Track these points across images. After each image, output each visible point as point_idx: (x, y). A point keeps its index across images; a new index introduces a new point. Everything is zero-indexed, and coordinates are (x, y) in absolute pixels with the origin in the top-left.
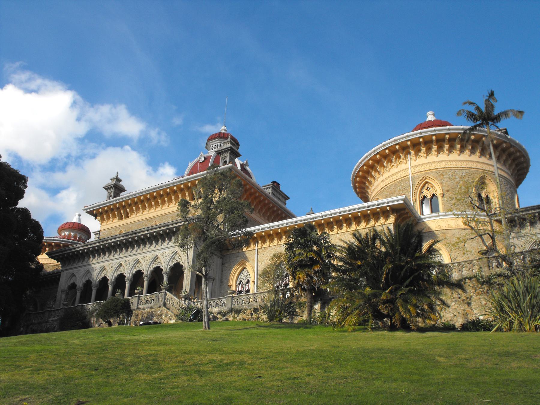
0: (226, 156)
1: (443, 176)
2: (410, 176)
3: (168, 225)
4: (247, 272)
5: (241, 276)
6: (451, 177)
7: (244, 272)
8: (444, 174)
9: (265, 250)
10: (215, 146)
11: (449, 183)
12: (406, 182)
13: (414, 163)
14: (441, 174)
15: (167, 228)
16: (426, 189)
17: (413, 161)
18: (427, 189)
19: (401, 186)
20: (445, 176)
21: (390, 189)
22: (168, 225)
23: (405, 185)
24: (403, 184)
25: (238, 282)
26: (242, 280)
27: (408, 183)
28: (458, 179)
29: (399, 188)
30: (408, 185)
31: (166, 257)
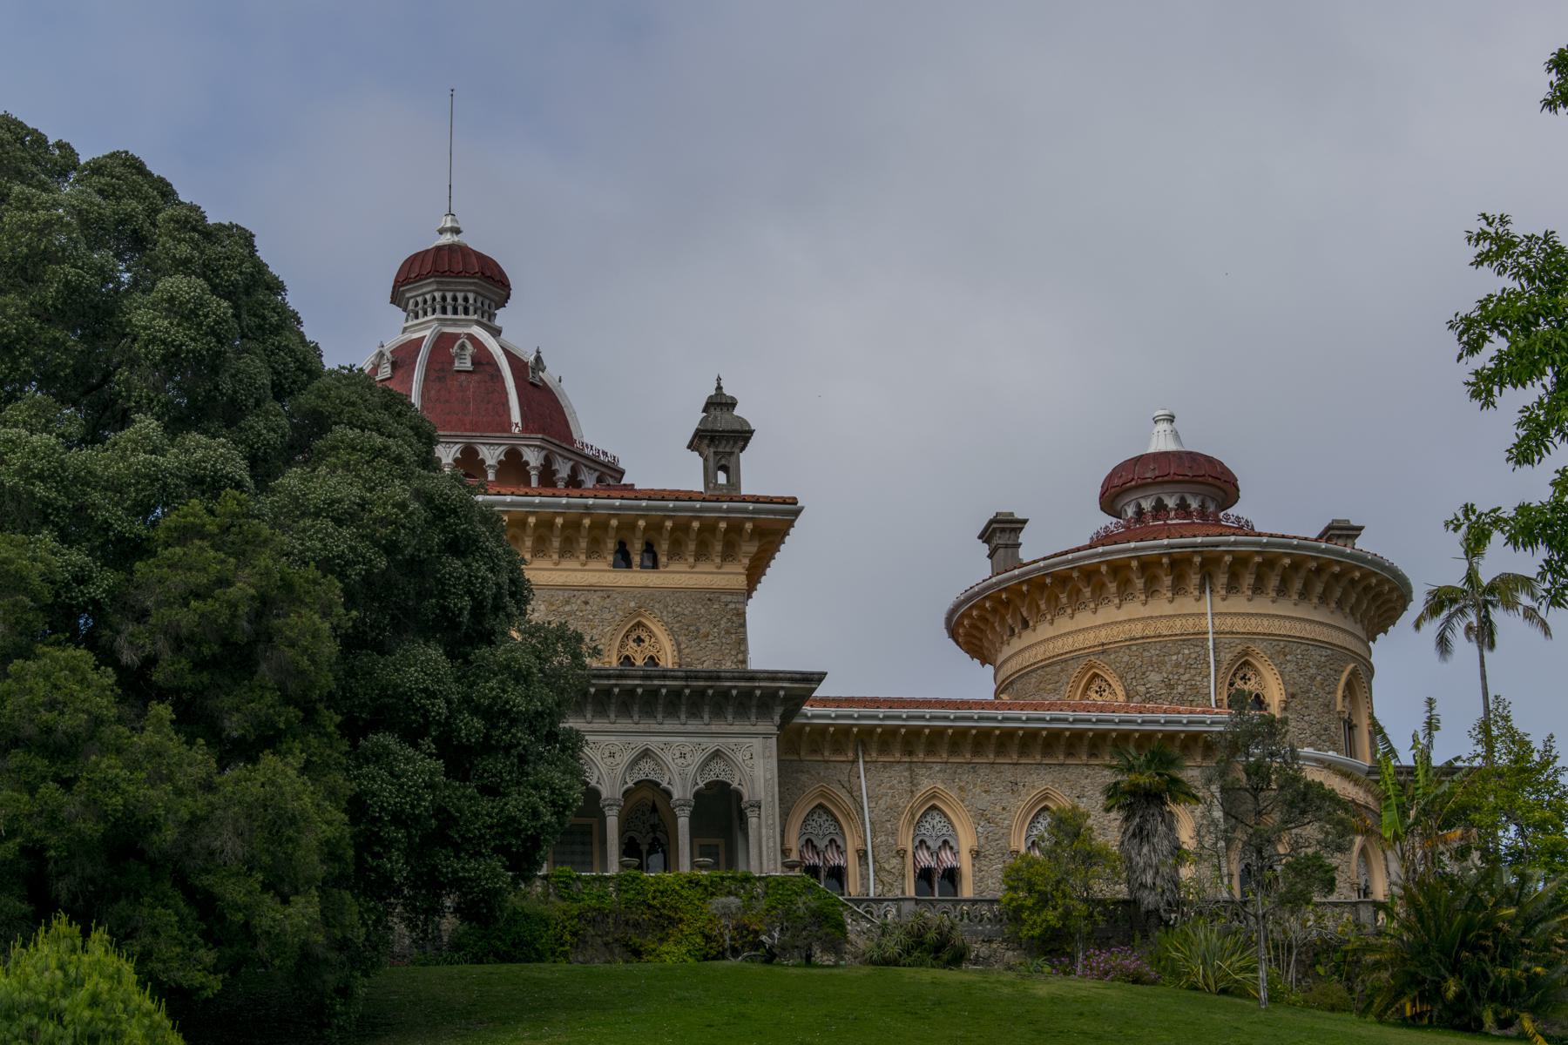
0: (728, 450)
1: (1285, 656)
2: (1210, 636)
3: (719, 678)
5: (809, 827)
6: (1300, 661)
7: (815, 817)
8: (1287, 650)
9: (885, 767)
11: (1296, 675)
12: (1198, 649)
13: (1222, 607)
14: (1282, 647)
15: (713, 684)
16: (1241, 679)
17: (1217, 600)
20: (1288, 658)
21: (1146, 654)
22: (719, 678)
23: (1193, 656)
24: (1186, 652)
27: (1203, 652)
28: (1313, 671)
29: (1174, 657)
30: (1202, 657)
31: (682, 760)
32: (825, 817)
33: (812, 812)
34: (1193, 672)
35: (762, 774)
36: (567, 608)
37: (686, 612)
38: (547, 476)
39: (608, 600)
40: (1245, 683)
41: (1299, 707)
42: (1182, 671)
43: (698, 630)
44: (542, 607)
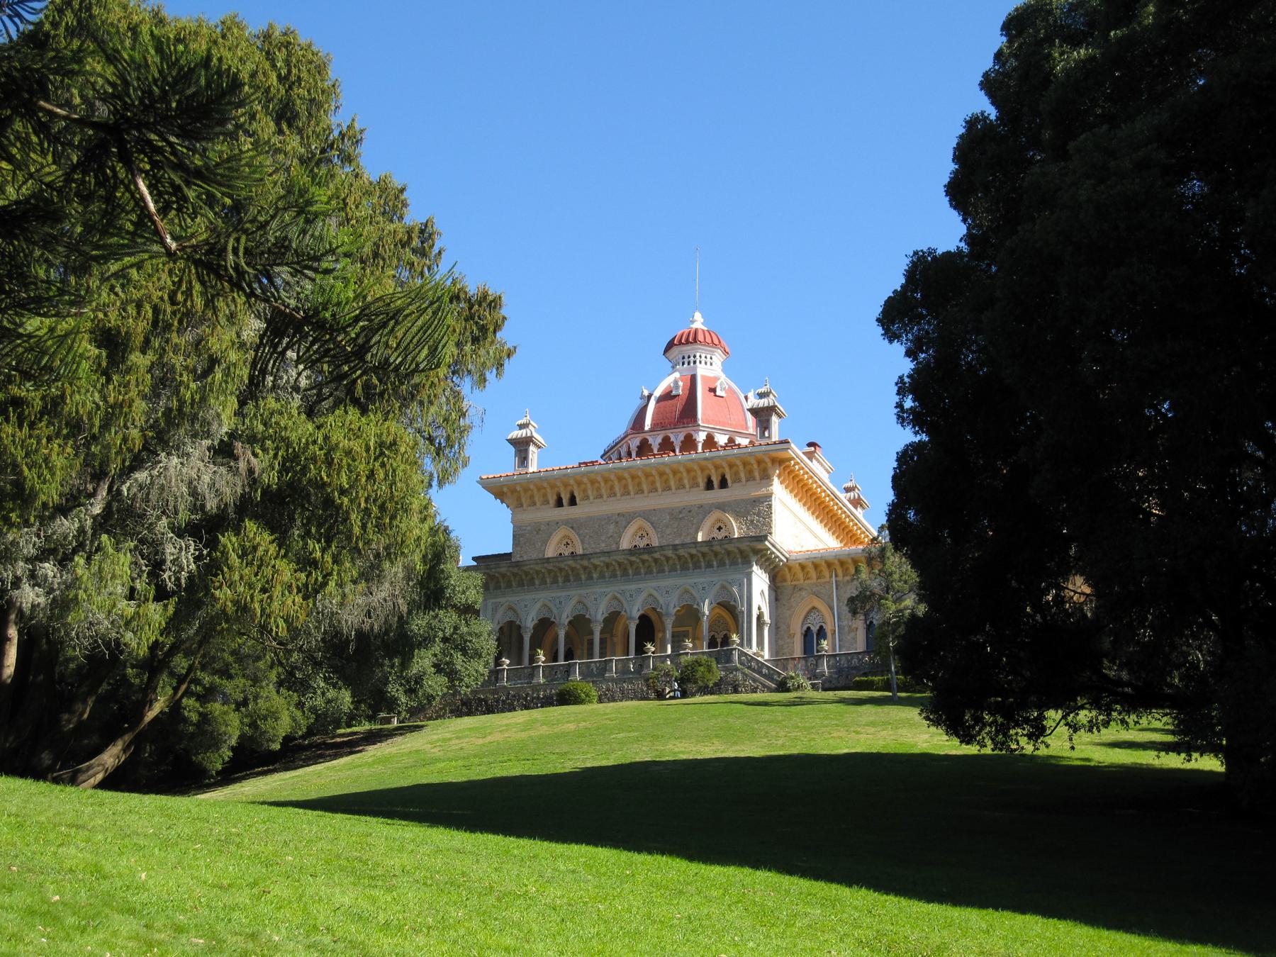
25: (805, 628)
36: (680, 516)
37: (742, 510)
38: (710, 442)
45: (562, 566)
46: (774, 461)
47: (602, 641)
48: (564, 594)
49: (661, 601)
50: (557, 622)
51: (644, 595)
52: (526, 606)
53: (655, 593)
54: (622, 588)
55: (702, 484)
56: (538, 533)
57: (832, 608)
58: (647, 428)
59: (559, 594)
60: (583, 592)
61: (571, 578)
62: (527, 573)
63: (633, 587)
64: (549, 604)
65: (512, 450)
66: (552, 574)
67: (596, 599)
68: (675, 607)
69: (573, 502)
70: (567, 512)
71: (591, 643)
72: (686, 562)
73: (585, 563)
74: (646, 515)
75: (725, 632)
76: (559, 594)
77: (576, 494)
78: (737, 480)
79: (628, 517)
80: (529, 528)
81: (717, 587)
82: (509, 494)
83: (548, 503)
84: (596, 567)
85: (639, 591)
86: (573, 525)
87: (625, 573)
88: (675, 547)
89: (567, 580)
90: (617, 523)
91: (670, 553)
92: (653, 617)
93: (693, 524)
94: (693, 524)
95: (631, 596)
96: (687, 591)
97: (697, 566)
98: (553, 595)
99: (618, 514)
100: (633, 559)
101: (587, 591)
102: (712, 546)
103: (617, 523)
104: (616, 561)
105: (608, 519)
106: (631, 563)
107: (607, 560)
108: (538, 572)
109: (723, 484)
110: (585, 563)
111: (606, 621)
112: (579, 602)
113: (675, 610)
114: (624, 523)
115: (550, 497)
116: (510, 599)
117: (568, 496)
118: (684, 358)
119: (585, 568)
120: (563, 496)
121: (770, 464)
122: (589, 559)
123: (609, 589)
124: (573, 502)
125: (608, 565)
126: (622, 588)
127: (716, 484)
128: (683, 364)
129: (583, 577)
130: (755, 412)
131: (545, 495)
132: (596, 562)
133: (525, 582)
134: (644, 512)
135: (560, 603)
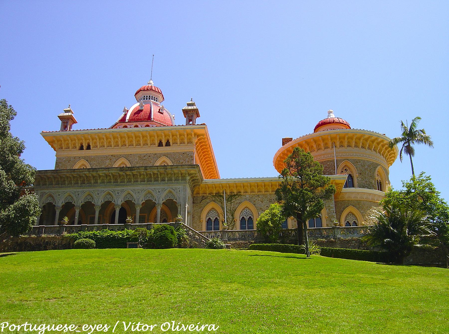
4: (214, 211)
5: (209, 214)
7: (212, 211)
10: (147, 96)
12: (331, 162)
16: (345, 170)
18: (346, 170)
19: (327, 165)
20: (359, 163)
25: (207, 218)
26: (211, 217)
28: (366, 167)
32: (214, 211)
33: (210, 210)
34: (330, 169)
35: (182, 196)
39: (156, 155)
40: (346, 171)
41: (362, 177)
42: (327, 169)
43: (180, 162)
44: (138, 158)
45: (81, 174)
46: (195, 134)
47: (99, 218)
48: (81, 190)
49: (135, 197)
50: (75, 204)
51: (126, 193)
52: (59, 195)
53: (132, 193)
54: (114, 189)
55: (157, 144)
56: (69, 162)
57: (223, 208)
58: (127, 121)
59: (78, 190)
60: (91, 189)
61: (86, 182)
62: (61, 177)
63: (120, 188)
64: (72, 195)
65: (60, 122)
66: (75, 179)
67: (98, 194)
68: (142, 200)
69: (89, 148)
70: (85, 153)
71: (94, 218)
72: (151, 177)
73: (94, 174)
74: (127, 157)
75: (165, 218)
76: (78, 190)
77: (91, 144)
78: (175, 143)
79: (118, 157)
80: (64, 159)
81: (167, 191)
82: (56, 142)
83: (76, 148)
84: (100, 176)
85: (122, 191)
86: (87, 159)
87: (116, 181)
88: (146, 168)
89: (83, 183)
90: (111, 159)
91: (142, 171)
92: (127, 207)
93: (150, 163)
94: (150, 163)
95: (118, 193)
96: (149, 193)
97: (156, 180)
98: (75, 190)
99: (112, 155)
100: (121, 173)
101: (94, 189)
102: (167, 169)
103: (111, 159)
104: (112, 174)
105: (106, 157)
106: (120, 176)
107: (107, 172)
108: (67, 177)
109: (168, 144)
110: (94, 174)
111: (102, 205)
112: (89, 195)
113: (142, 202)
114: (114, 160)
115: (77, 145)
116: (51, 191)
117: (87, 145)
118: (144, 97)
119: (94, 177)
120: (84, 145)
121: (193, 136)
122: (97, 171)
123: (106, 189)
124: (89, 148)
125: (107, 176)
126: (114, 189)
127: (164, 144)
128: (144, 99)
129: (92, 182)
130: (186, 112)
131: (74, 144)
132: (101, 173)
133: (60, 182)
134: (125, 155)
135: (78, 194)
